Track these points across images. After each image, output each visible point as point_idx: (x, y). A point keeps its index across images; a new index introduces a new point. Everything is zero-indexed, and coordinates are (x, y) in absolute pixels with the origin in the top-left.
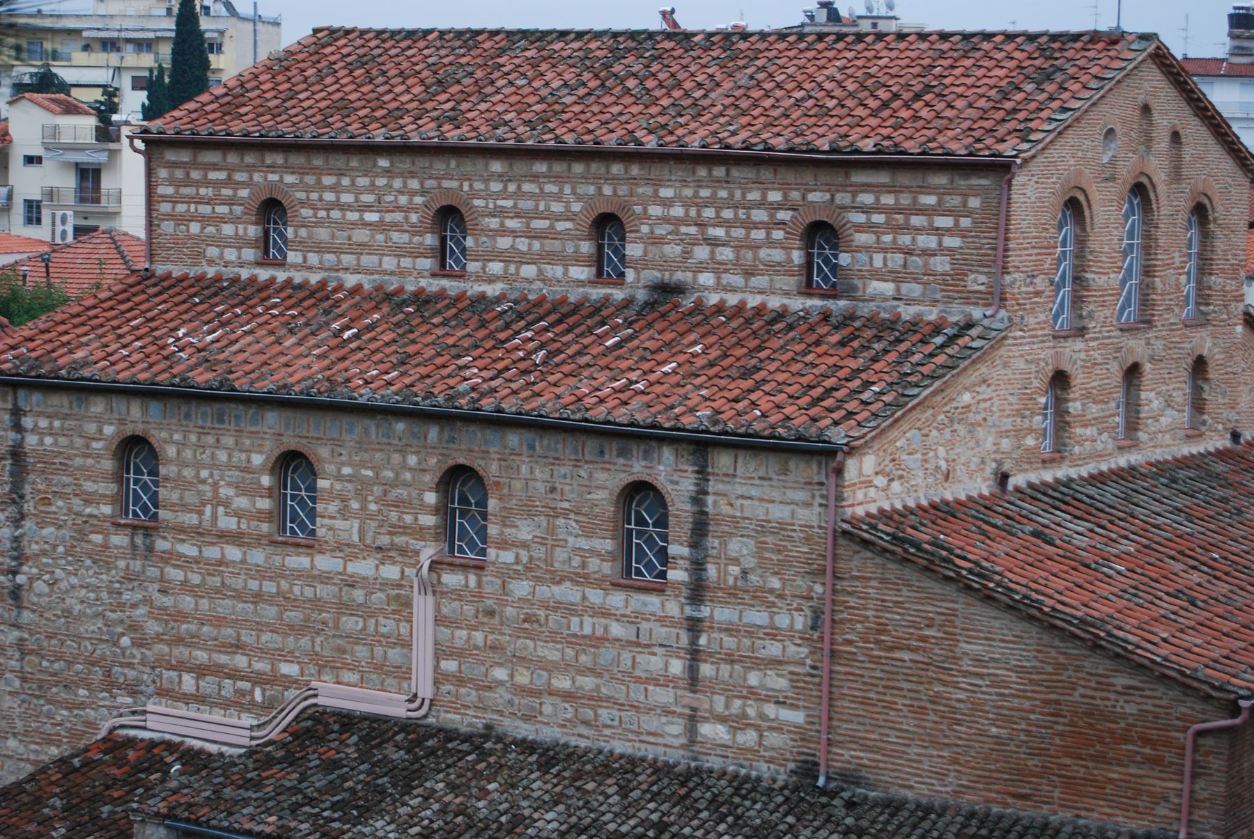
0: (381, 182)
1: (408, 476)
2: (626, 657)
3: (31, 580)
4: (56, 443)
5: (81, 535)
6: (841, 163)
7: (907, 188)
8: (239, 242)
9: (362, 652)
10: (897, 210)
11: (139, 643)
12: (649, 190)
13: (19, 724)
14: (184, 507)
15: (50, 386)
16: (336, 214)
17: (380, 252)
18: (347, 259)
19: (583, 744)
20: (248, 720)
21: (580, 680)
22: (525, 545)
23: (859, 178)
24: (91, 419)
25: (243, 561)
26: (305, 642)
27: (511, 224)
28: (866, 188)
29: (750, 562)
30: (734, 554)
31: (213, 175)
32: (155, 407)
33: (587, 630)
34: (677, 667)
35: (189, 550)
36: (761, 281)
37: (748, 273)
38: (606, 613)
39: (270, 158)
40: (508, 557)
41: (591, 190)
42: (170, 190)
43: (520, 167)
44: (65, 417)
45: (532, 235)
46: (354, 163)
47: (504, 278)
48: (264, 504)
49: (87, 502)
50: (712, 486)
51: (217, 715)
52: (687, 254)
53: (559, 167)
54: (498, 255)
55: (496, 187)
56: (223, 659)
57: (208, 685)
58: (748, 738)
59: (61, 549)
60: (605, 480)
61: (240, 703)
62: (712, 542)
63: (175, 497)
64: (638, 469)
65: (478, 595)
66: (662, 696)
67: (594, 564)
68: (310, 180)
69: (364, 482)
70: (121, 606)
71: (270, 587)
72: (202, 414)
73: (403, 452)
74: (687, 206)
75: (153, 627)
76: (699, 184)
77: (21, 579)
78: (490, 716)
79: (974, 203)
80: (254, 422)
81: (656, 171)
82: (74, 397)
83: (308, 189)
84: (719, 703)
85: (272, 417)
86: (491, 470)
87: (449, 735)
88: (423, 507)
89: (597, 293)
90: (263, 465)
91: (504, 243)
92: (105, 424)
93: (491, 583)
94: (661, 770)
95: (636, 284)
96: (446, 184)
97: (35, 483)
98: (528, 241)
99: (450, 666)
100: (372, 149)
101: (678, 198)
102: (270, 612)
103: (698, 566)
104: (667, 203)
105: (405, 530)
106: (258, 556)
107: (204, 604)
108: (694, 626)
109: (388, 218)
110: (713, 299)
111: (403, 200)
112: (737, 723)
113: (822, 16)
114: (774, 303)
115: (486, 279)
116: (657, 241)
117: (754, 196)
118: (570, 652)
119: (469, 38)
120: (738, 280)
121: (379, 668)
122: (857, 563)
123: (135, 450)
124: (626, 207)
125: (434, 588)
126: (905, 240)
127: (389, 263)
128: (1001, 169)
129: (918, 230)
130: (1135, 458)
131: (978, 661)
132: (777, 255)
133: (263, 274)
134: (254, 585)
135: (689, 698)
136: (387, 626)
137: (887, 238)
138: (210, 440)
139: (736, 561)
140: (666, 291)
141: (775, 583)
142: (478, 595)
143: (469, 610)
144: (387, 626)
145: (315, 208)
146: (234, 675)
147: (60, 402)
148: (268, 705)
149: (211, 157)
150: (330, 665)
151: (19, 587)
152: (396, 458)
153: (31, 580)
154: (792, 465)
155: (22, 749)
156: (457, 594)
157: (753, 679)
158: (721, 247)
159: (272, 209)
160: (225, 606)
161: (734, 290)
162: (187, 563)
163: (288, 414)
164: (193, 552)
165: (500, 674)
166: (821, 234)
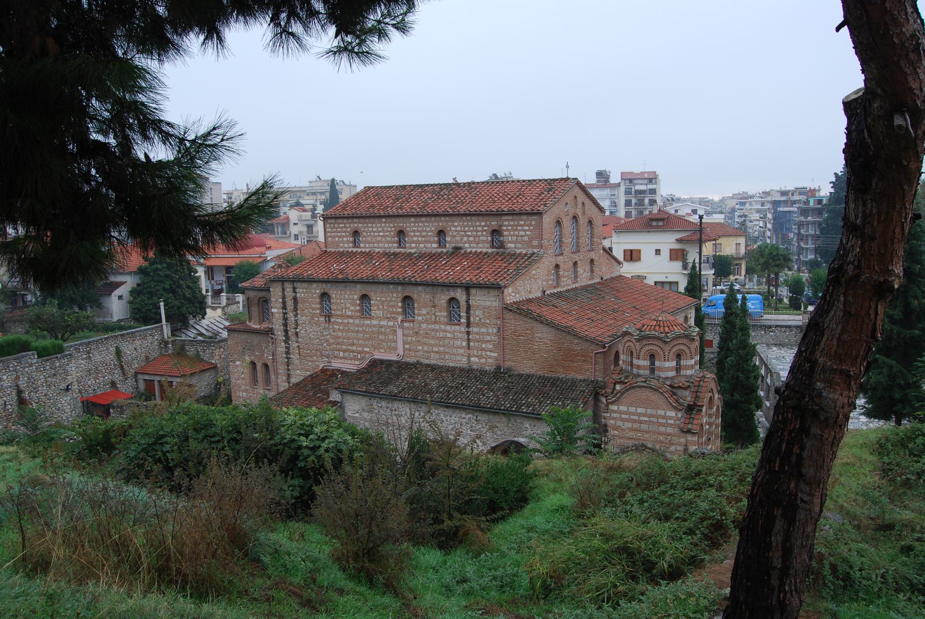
2: (451, 342)
5: (312, 318)
6: (499, 214)
8: (348, 242)
9: (385, 344)
15: (302, 281)
20: (357, 363)
23: (504, 218)
28: (506, 220)
30: (477, 315)
32: (329, 285)
34: (464, 344)
36: (481, 245)
37: (477, 244)
40: (420, 318)
43: (418, 219)
47: (416, 247)
48: (358, 308)
51: (349, 362)
57: (346, 354)
58: (483, 361)
60: (443, 298)
61: (355, 358)
62: (472, 312)
64: (452, 294)
66: (461, 351)
71: (360, 329)
72: (341, 286)
75: (332, 341)
79: (533, 223)
81: (453, 219)
85: (359, 286)
86: (415, 296)
87: (407, 364)
89: (439, 250)
91: (415, 239)
92: (317, 290)
94: (462, 370)
95: (449, 247)
97: (300, 306)
98: (422, 237)
99: (407, 346)
100: (380, 217)
103: (468, 318)
104: (456, 227)
105: (394, 313)
106: (357, 321)
108: (468, 333)
110: (469, 250)
112: (480, 357)
114: (484, 250)
119: (404, 187)
120: (475, 245)
122: (508, 315)
123: (324, 296)
125: (402, 327)
126: (516, 233)
127: (386, 245)
128: (539, 214)
130: (577, 285)
131: (540, 338)
132: (484, 238)
133: (355, 250)
140: (457, 249)
144: (391, 337)
146: (353, 352)
147: (305, 285)
148: (362, 359)
149: (340, 221)
156: (408, 328)
157: (484, 346)
158: (472, 237)
159: (356, 233)
160: (349, 334)
162: (339, 324)
165: (420, 348)
166: (496, 232)
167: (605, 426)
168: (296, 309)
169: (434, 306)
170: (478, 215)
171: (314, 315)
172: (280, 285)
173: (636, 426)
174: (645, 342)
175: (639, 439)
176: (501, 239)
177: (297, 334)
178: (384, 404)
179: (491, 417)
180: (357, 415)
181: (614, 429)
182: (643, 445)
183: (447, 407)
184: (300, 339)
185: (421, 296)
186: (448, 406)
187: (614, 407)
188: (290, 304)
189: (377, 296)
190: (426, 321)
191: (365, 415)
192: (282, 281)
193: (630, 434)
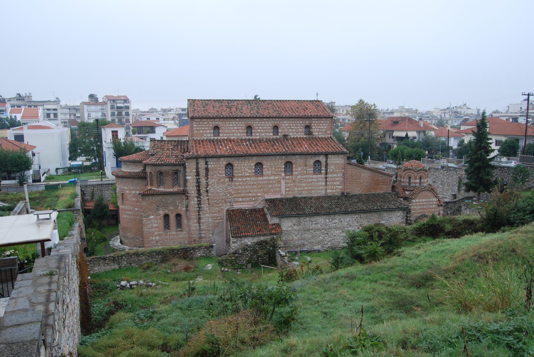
2: (316, 183)
5: (220, 180)
9: (272, 190)
11: (231, 195)
13: (208, 212)
14: (239, 173)
15: (213, 157)
17: (237, 133)
18: (231, 135)
20: (252, 203)
26: (262, 190)
30: (331, 168)
32: (233, 159)
34: (324, 184)
35: (240, 179)
36: (299, 134)
38: (312, 178)
39: (216, 120)
40: (297, 173)
43: (261, 120)
46: (232, 120)
47: (259, 136)
51: (246, 203)
53: (268, 119)
54: (258, 132)
55: (257, 123)
57: (244, 199)
58: (334, 191)
60: (311, 161)
62: (328, 167)
63: (237, 172)
64: (317, 158)
66: (322, 188)
67: (311, 172)
69: (272, 166)
73: (278, 160)
74: (288, 124)
75: (233, 192)
81: (283, 119)
83: (223, 124)
84: (330, 187)
85: (255, 158)
86: (293, 161)
88: (282, 168)
92: (223, 162)
93: (294, 177)
94: (325, 197)
97: (210, 173)
98: (263, 130)
99: (288, 189)
102: (255, 187)
103: (326, 170)
105: (279, 171)
106: (253, 179)
107: (243, 187)
108: (326, 178)
110: (293, 137)
112: (332, 189)
113: (18, 96)
114: (302, 136)
115: (256, 136)
116: (284, 129)
123: (230, 166)
127: (239, 135)
132: (302, 130)
133: (216, 138)
135: (325, 187)
136: (276, 185)
140: (285, 136)
143: (290, 181)
144: (276, 185)
146: (249, 197)
147: (215, 159)
150: (267, 193)
156: (288, 179)
157: (335, 183)
158: (294, 130)
159: (216, 128)
160: (247, 187)
162: (240, 181)
165: (296, 189)
166: (308, 127)
167: (410, 209)
168: (207, 175)
169: (306, 166)
170: (299, 118)
171: (222, 178)
172: (194, 161)
173: (422, 207)
174: (419, 172)
176: (311, 130)
177: (207, 191)
178: (307, 219)
180: (290, 229)
182: (424, 215)
183: (345, 214)
184: (209, 194)
185: (297, 161)
186: (346, 213)
187: (414, 201)
188: (202, 172)
189: (267, 164)
190: (301, 174)
191: (295, 227)
192: (197, 158)
193: (420, 211)
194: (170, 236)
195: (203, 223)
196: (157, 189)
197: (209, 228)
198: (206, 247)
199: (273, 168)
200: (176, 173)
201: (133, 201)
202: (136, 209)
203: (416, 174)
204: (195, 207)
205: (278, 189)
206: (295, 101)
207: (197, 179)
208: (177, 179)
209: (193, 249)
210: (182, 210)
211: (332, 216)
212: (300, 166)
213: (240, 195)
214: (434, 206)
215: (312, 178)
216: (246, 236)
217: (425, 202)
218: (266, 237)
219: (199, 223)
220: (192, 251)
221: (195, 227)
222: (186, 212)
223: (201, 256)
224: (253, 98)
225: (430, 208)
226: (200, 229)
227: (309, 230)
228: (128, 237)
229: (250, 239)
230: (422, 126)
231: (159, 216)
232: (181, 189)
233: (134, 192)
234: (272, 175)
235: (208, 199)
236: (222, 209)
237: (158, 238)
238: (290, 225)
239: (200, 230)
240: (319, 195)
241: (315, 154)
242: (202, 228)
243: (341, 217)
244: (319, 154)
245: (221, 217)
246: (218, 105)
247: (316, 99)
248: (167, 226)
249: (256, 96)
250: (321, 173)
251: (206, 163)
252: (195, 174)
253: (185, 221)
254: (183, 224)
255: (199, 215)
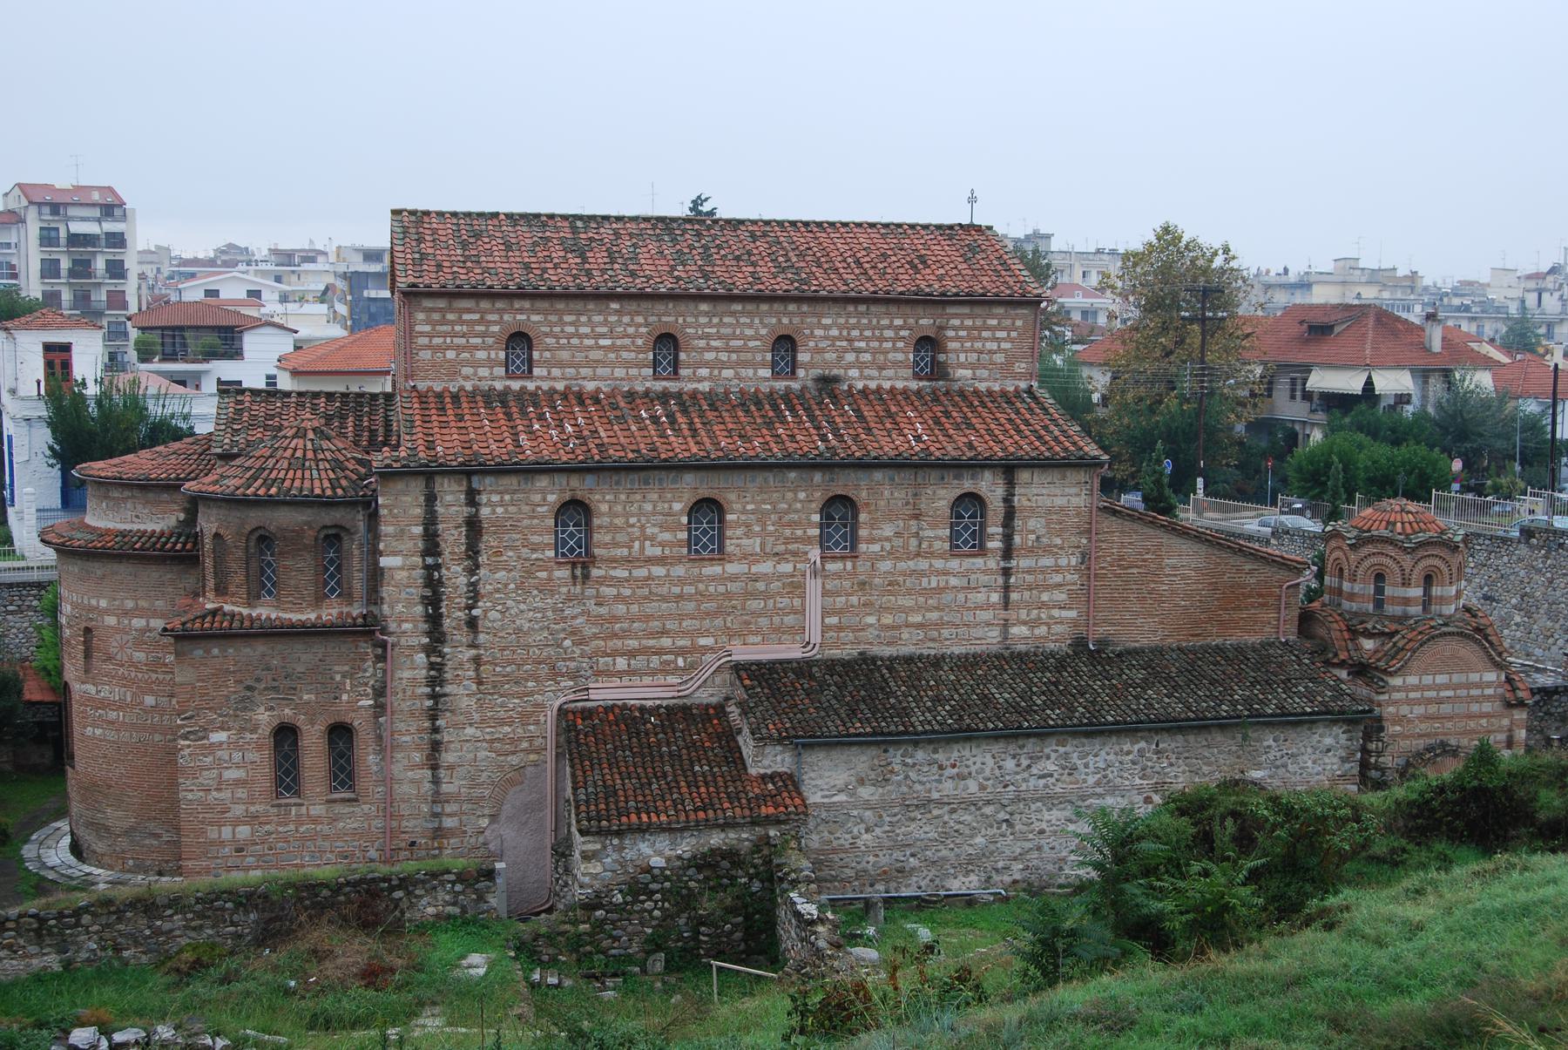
0: (613, 319)
1: (799, 506)
2: (961, 597)
3: (485, 612)
4: (506, 511)
5: (529, 573)
7: (980, 316)
9: (763, 622)
10: (974, 328)
12: (815, 320)
13: (476, 717)
14: (616, 545)
15: (501, 470)
16: (575, 341)
17: (612, 365)
18: (584, 371)
19: (933, 652)
20: (671, 679)
21: (929, 615)
22: (888, 539)
23: (951, 310)
24: (536, 492)
25: (667, 575)
26: (719, 622)
27: (714, 343)
28: (956, 316)
29: (1043, 531)
30: (1030, 528)
31: (466, 317)
32: (590, 480)
33: (934, 585)
34: (995, 597)
35: (621, 573)
36: (890, 373)
37: (881, 368)
38: (946, 573)
39: (517, 304)
40: (876, 548)
41: (774, 320)
42: (428, 328)
43: (721, 307)
44: (514, 492)
45: (730, 351)
46: (591, 306)
47: (710, 378)
49: (534, 550)
50: (1018, 490)
51: (647, 680)
52: (840, 358)
53: (750, 307)
54: (706, 364)
55: (703, 320)
56: (651, 643)
58: (1043, 630)
59: (512, 586)
61: (665, 670)
62: (1018, 523)
63: (608, 538)
65: (854, 573)
67: (937, 545)
68: (553, 318)
69: (766, 513)
70: (564, 619)
72: (628, 481)
74: (840, 328)
75: (589, 631)
76: (849, 315)
77: (475, 612)
78: (862, 647)
79: (1019, 323)
80: (674, 481)
81: (819, 308)
82: (521, 478)
84: (1023, 615)
85: (689, 478)
86: (862, 496)
88: (811, 524)
90: (681, 513)
91: (710, 356)
92: (548, 494)
93: (863, 567)
94: (999, 656)
95: (805, 377)
96: (664, 319)
97: (488, 541)
98: (727, 354)
99: (834, 620)
101: (835, 324)
102: (690, 606)
103: (1008, 538)
104: (826, 328)
105: (796, 540)
106: (679, 571)
107: (635, 608)
108: (1006, 572)
109: (619, 342)
110: (860, 385)
111: (631, 330)
112: (1032, 624)
114: (900, 385)
115: (696, 379)
117: (885, 322)
118: (922, 599)
120: (875, 373)
121: (777, 630)
123: (575, 511)
124: (799, 331)
126: (978, 345)
129: (986, 339)
131: (1174, 568)
132: (900, 357)
133: (516, 385)
134: (677, 590)
135: (1003, 614)
136: (784, 602)
137: (968, 345)
138: (638, 497)
139: (1033, 532)
140: (827, 383)
141: (1058, 541)
142: (854, 573)
144: (784, 602)
145: (557, 338)
146: (659, 652)
147: (511, 482)
148: (691, 667)
151: (476, 617)
152: (790, 495)
153: (485, 612)
154: (1068, 474)
155: (479, 733)
156: (838, 575)
157: (1045, 597)
159: (519, 340)
160: (652, 607)
161: (872, 379)
162: (620, 582)
163: (703, 474)
164: (626, 574)
165: (871, 620)
166: (928, 344)
167: (1380, 719)
168: (472, 551)
169: (917, 517)
170: (887, 301)
171: (542, 565)
173: (1432, 709)
174: (1421, 553)
175: (1436, 734)
176: (942, 357)
177: (472, 623)
178: (920, 755)
179: (1191, 738)
180: (842, 797)
181: (1394, 723)
182: (1443, 744)
183: (1088, 735)
184: (482, 638)
185: (880, 498)
186: (1094, 730)
187: (1396, 681)
188: (453, 538)
189: (745, 505)
190: (892, 554)
191: (865, 792)
192: (429, 474)
193: (1423, 727)
194: (299, 823)
195: (451, 768)
196: (245, 611)
197: (477, 792)
198: (461, 878)
199: (769, 525)
200: (334, 538)
201: (134, 664)
202: (150, 700)
203: (1407, 561)
204: (414, 696)
205: (790, 620)
206: (872, 225)
207: (426, 567)
208: (339, 569)
209: (406, 883)
210: (356, 705)
211: (1031, 745)
212: (891, 517)
213: (619, 643)
214: (1487, 707)
215: (946, 573)
216: (642, 830)
217: (1447, 687)
218: (732, 835)
219: (435, 768)
220: (398, 894)
221: (416, 782)
222: (376, 717)
223: (438, 916)
224: (683, 211)
225: (1470, 717)
226: (437, 793)
227: (925, 804)
228: (107, 829)
229: (663, 842)
230: (1437, 346)
231: (254, 730)
232: (356, 610)
233: (139, 623)
234: (765, 555)
235: (477, 661)
236: (541, 706)
237: (244, 831)
238: (840, 783)
239: (437, 798)
240: (972, 649)
241: (957, 467)
242: (445, 788)
243: (1073, 749)
244: (976, 465)
245: (531, 739)
246: (527, 235)
247: (966, 221)
248: (287, 777)
249: (697, 203)
250: (981, 551)
251: (472, 498)
252: (421, 545)
253: (368, 759)
254: (360, 770)
255: (436, 730)
